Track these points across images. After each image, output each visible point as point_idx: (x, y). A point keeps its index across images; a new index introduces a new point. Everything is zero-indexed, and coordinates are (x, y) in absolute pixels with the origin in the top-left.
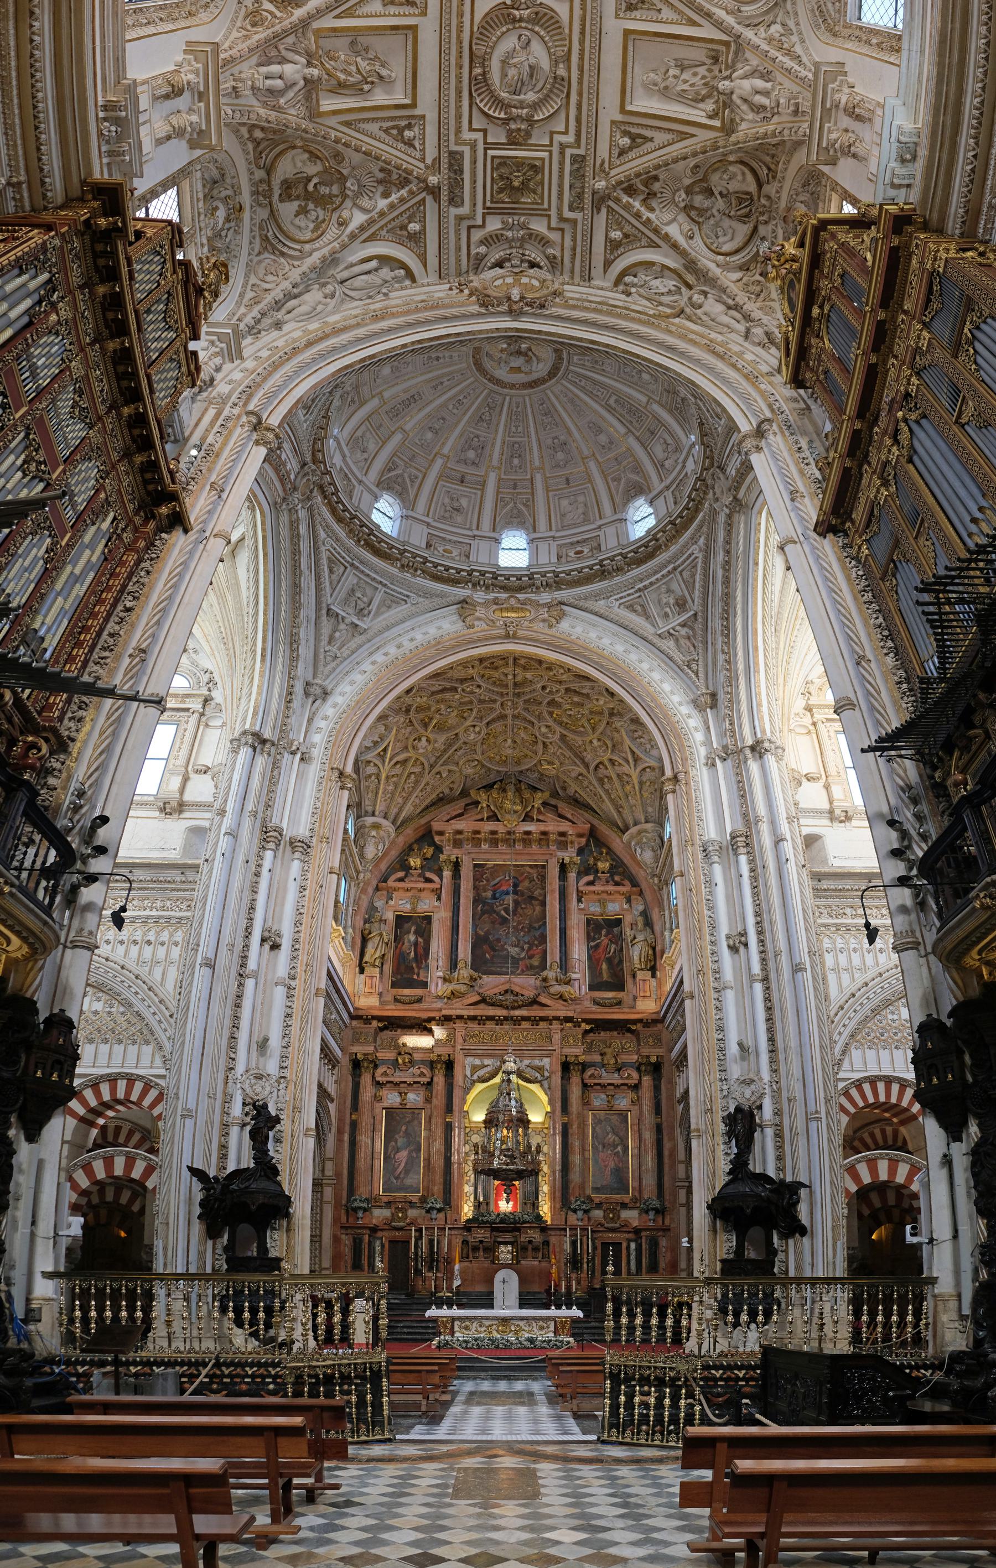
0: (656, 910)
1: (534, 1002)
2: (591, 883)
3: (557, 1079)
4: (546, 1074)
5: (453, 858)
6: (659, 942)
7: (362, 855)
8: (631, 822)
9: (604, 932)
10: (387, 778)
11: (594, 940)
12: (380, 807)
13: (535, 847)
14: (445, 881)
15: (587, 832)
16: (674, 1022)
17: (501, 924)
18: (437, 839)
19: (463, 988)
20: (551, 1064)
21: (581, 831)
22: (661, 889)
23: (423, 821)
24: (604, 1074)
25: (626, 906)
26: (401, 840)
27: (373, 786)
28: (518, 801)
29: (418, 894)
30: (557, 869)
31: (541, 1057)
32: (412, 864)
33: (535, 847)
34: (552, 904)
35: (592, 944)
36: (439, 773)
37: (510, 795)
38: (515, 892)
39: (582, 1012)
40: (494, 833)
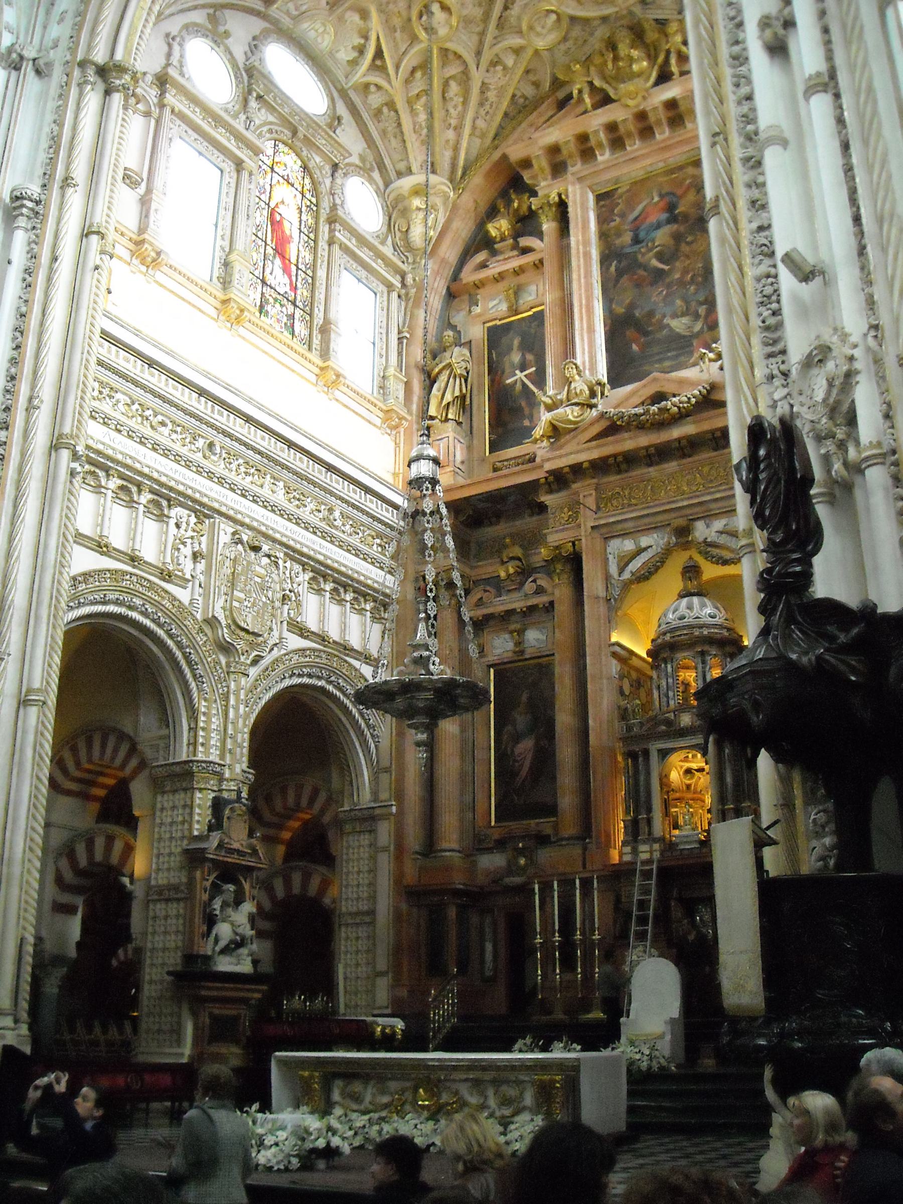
5: (554, 197)
7: (405, 247)
10: (408, 102)
12: (417, 156)
14: (546, 238)
17: (652, 285)
18: (526, 176)
19: (571, 413)
23: (497, 155)
26: (467, 200)
27: (391, 127)
28: (635, 53)
29: (514, 281)
32: (493, 233)
36: (494, 64)
37: (623, 49)
38: (673, 219)
40: (612, 127)
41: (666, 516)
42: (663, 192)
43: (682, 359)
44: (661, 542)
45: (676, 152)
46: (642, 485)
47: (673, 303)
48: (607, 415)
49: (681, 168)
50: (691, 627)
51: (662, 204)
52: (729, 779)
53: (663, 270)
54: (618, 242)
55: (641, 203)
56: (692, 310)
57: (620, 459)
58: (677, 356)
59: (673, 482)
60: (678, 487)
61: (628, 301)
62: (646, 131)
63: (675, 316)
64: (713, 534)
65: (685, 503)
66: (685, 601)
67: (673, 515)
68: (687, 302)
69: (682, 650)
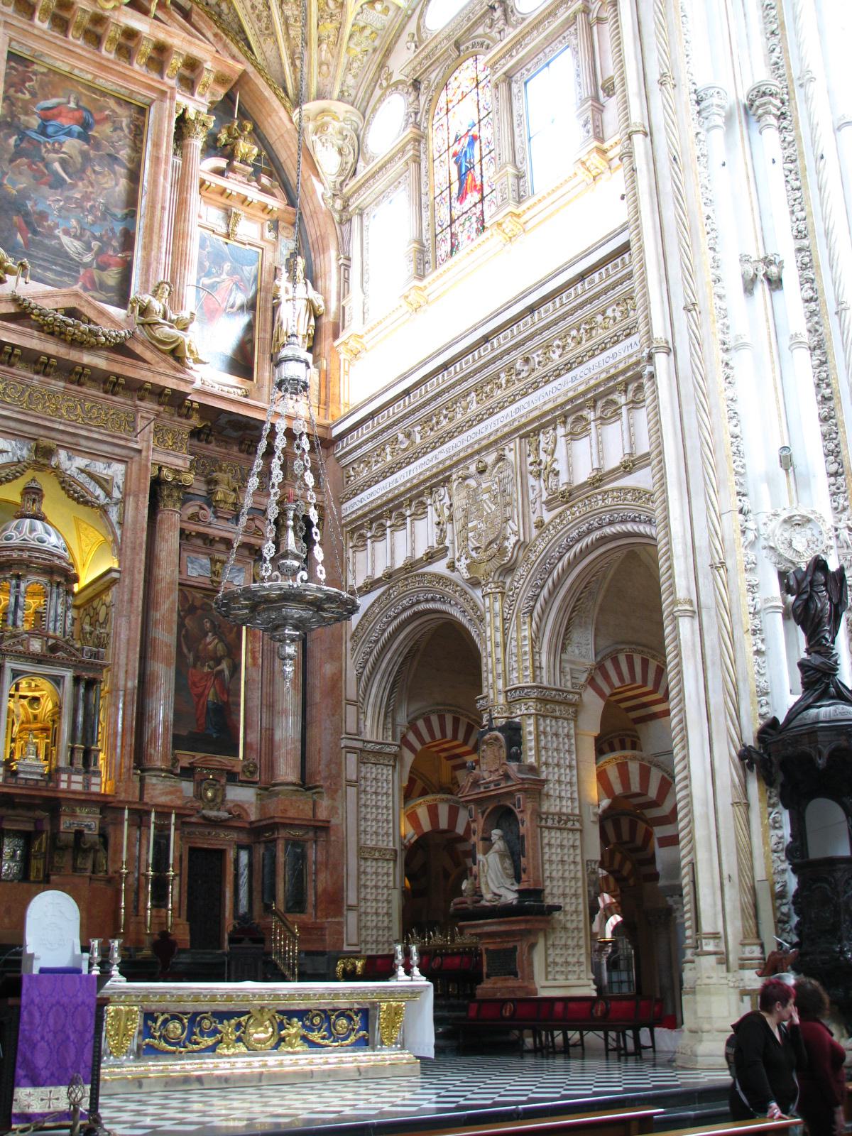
0: (333, 253)
1: (121, 349)
2: (220, 172)
3: (138, 510)
4: (116, 494)
6: (333, 306)
8: (313, 90)
9: (227, 266)
11: (208, 274)
13: (138, 66)
15: (236, 77)
16: (365, 448)
17: (51, 187)
20: (126, 475)
21: (227, 72)
22: (345, 221)
24: (211, 518)
25: (270, 236)
30: (174, 124)
31: (110, 458)
33: (138, 66)
34: (154, 182)
35: (206, 281)
38: (84, 137)
39: (201, 392)
41: (33, 430)
42: (81, 104)
43: (66, 279)
44: (19, 452)
45: (111, 78)
46: (20, 387)
47: (67, 219)
48: (26, 304)
49: (104, 94)
50: (53, 554)
51: (77, 114)
52: (80, 719)
53: (64, 180)
54: (23, 118)
55: (54, 96)
56: (85, 239)
57: (17, 351)
58: (60, 274)
59: (53, 401)
60: (57, 408)
61: (22, 186)
62: (95, 39)
63: (67, 232)
64: (73, 469)
65: (62, 427)
66: (38, 523)
67: (42, 432)
68: (83, 229)
69: (38, 574)
